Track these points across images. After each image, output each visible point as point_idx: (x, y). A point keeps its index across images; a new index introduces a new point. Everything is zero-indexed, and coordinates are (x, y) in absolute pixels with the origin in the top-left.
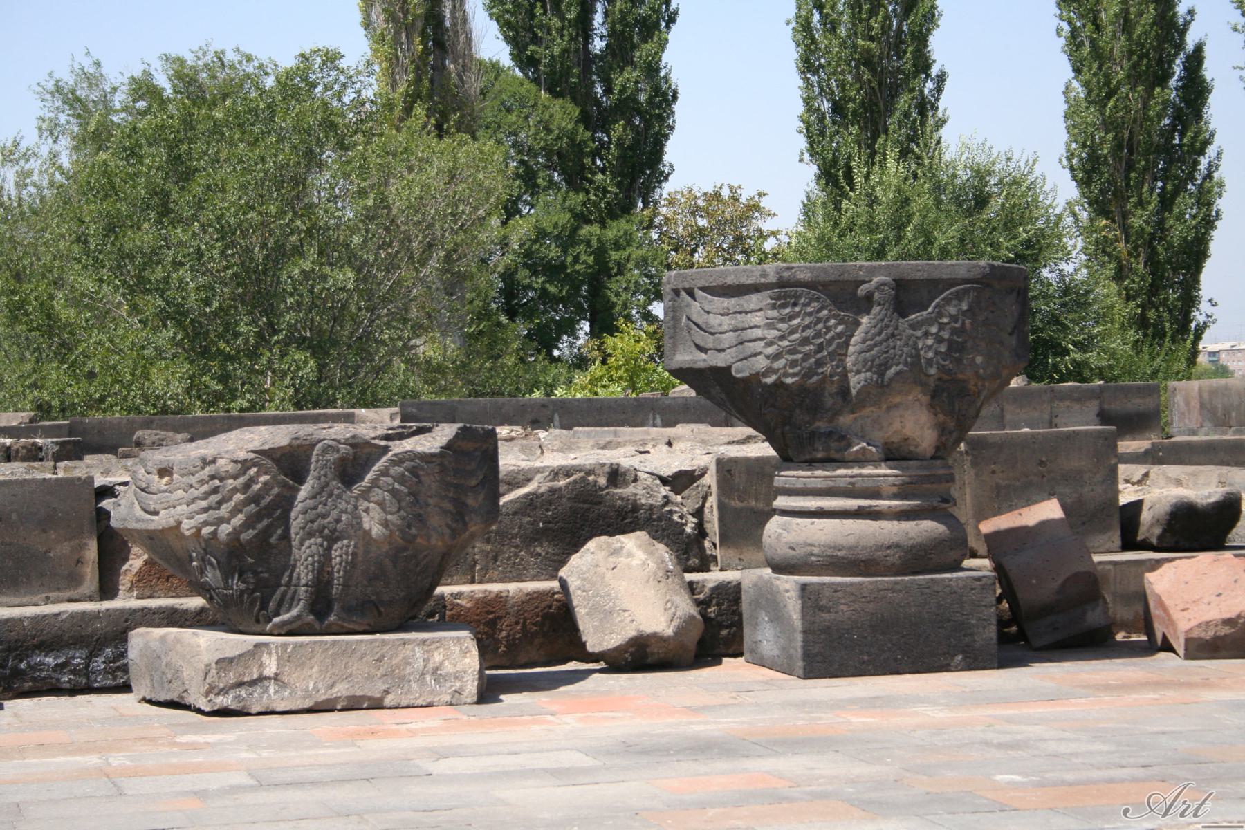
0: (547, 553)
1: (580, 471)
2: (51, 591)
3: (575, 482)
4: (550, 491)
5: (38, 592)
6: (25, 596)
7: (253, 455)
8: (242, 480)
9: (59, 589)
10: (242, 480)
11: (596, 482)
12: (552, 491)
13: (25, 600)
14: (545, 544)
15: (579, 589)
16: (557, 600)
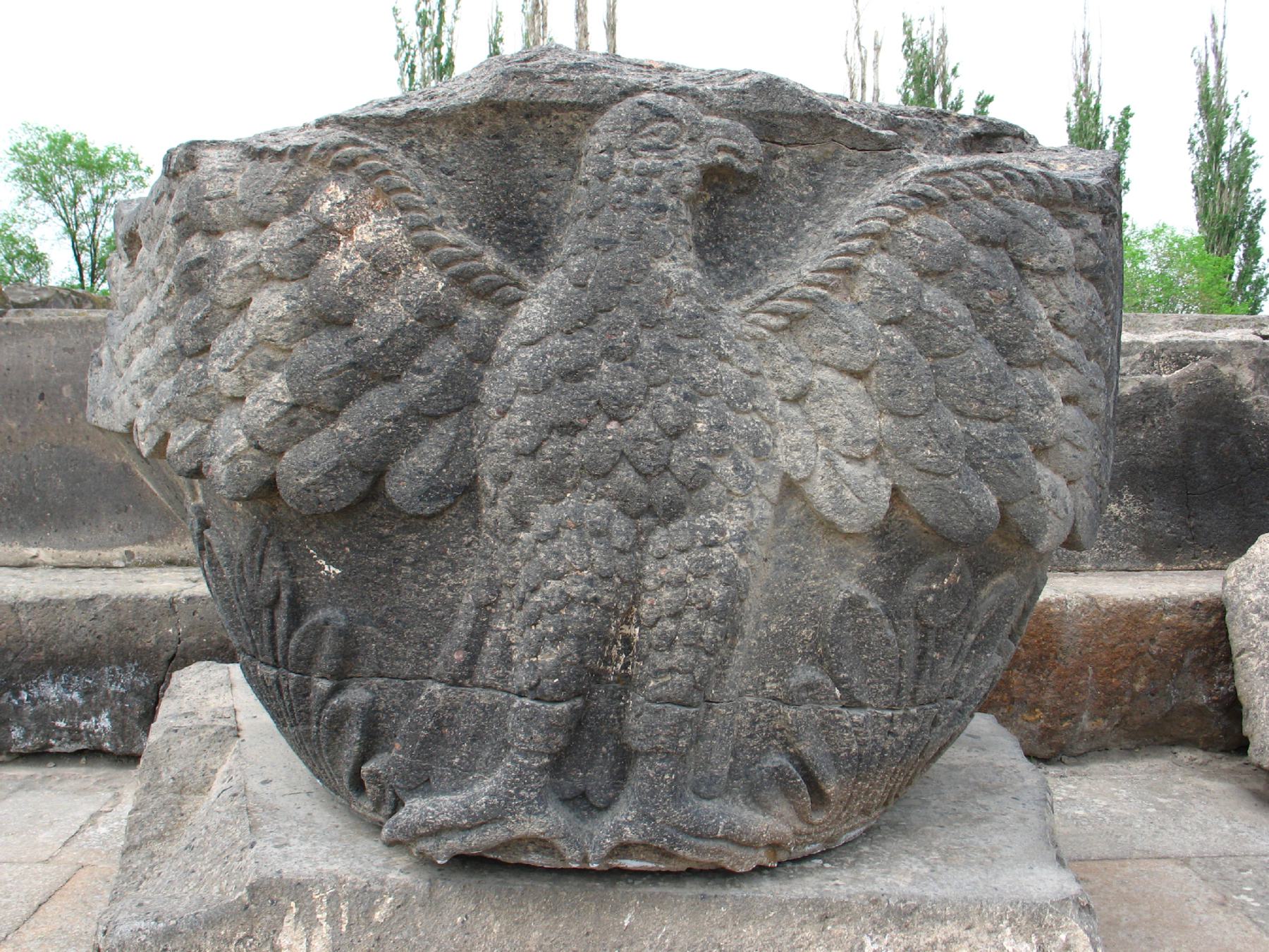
0: (1129, 517)
1: (1206, 354)
2: (134, 544)
3: (1193, 376)
4: (1145, 392)
5: (112, 544)
6: (87, 548)
7: (335, 135)
8: (281, 231)
9: (151, 539)
10: (281, 231)
11: (1235, 377)
12: (1147, 391)
13: (91, 555)
14: (1127, 496)
15: (1258, 610)
16: (1168, 627)
